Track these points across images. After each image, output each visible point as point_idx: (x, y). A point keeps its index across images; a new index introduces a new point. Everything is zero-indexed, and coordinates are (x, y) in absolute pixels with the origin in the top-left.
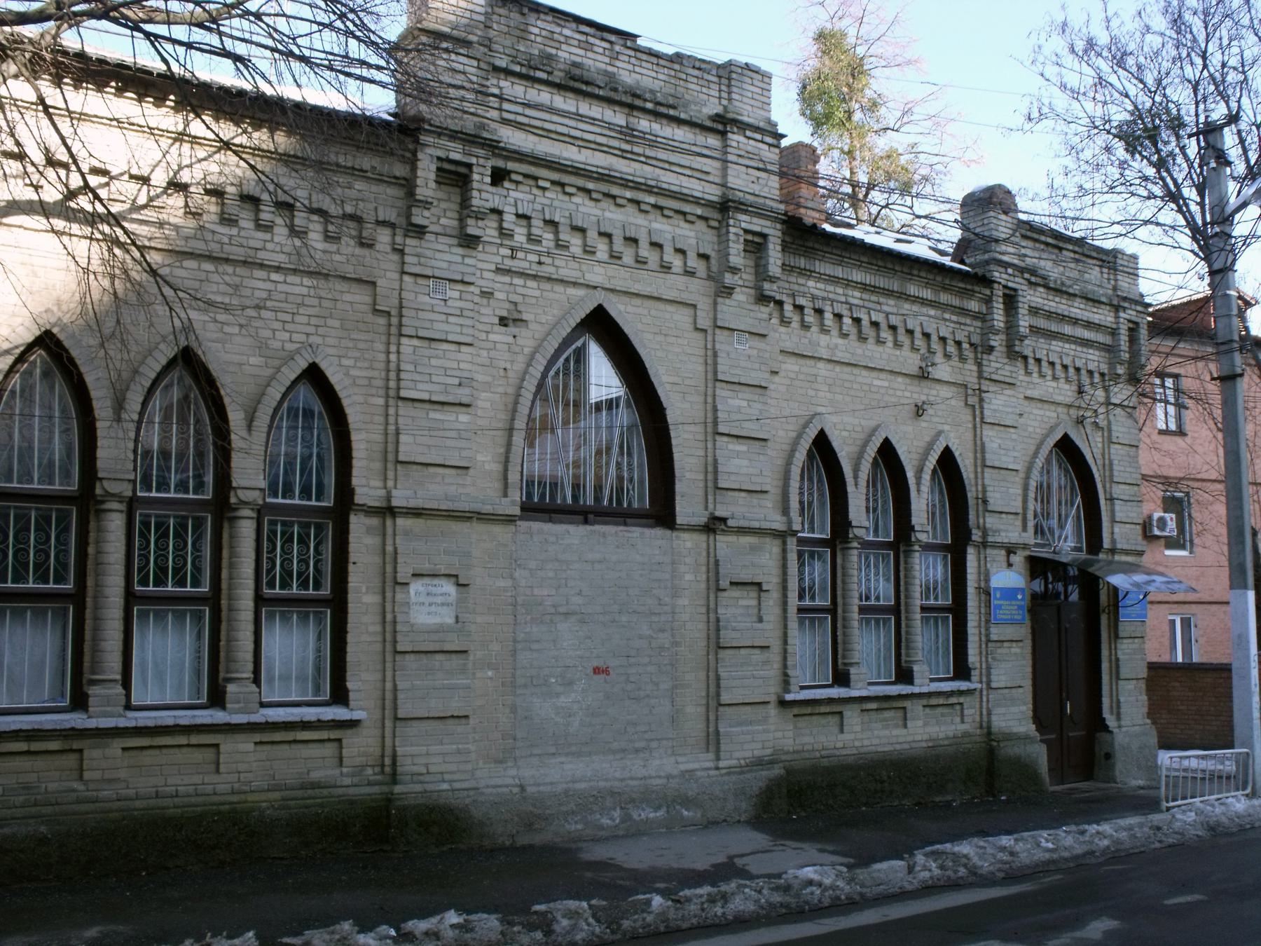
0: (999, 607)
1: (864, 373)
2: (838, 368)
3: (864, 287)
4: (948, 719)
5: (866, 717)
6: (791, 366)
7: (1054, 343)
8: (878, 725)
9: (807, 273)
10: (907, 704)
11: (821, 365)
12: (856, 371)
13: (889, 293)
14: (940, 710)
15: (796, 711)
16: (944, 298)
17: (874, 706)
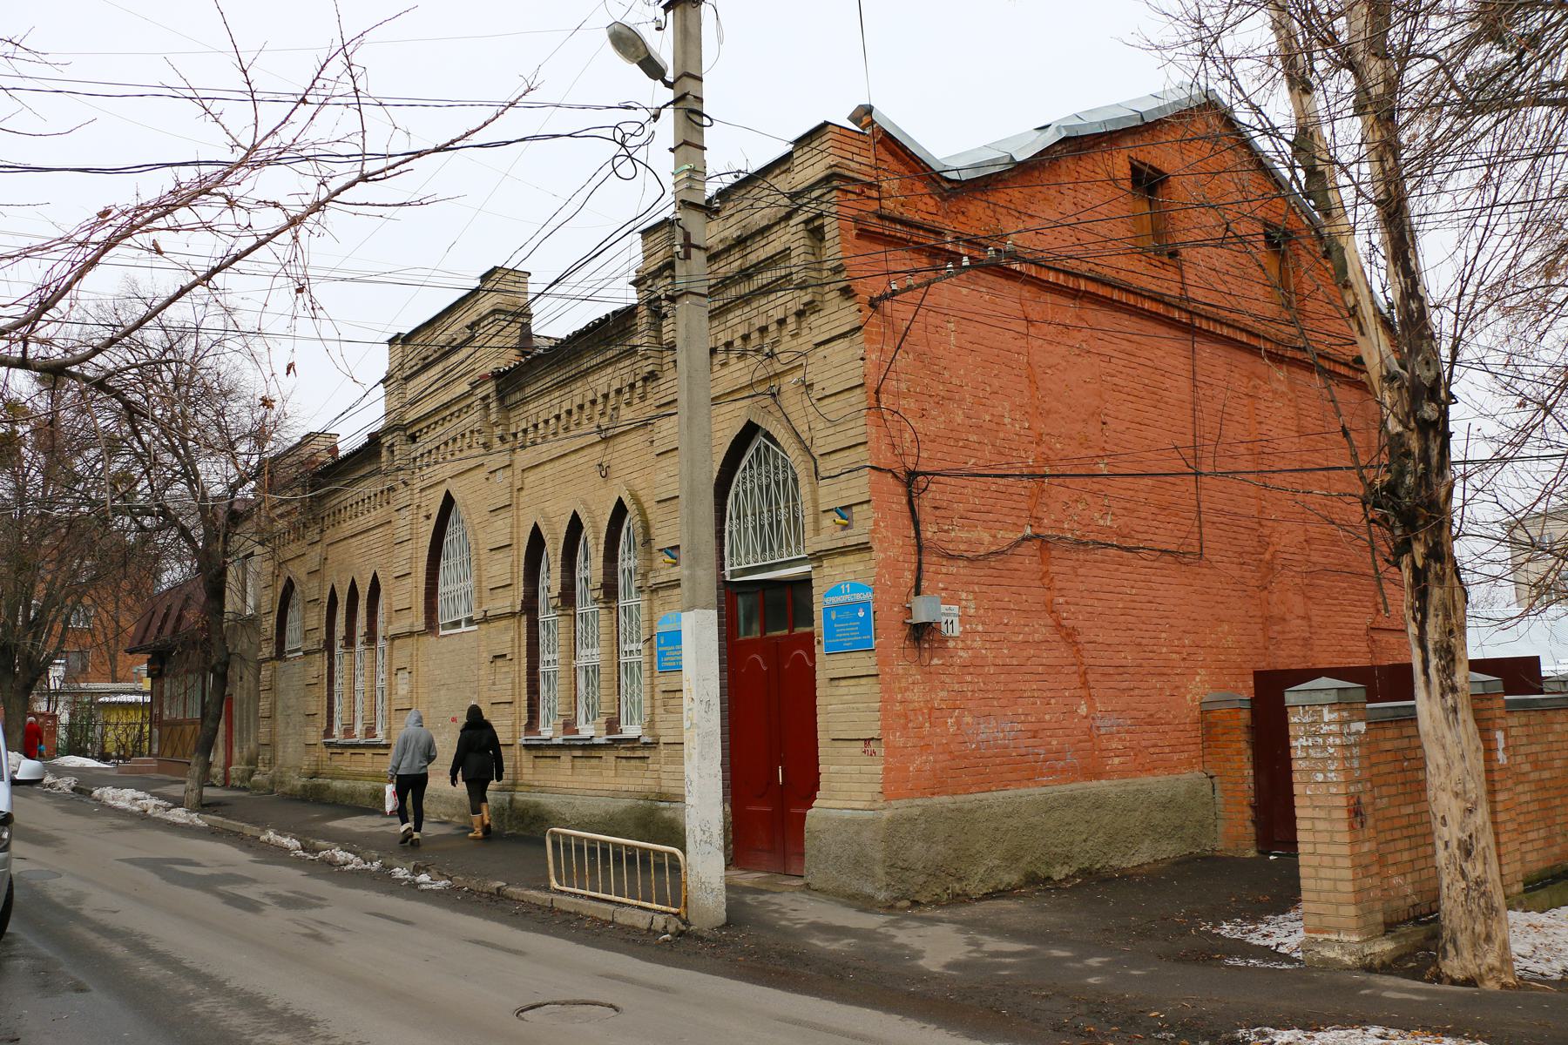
0: (662, 654)
1: (573, 457)
2: (557, 463)
3: (560, 385)
4: (640, 773)
5: (578, 763)
6: (532, 477)
7: (730, 316)
8: (586, 771)
9: (524, 401)
10: (602, 754)
11: (547, 467)
12: (567, 459)
13: (574, 379)
14: (633, 762)
15: (534, 753)
16: (610, 354)
17: (578, 753)
